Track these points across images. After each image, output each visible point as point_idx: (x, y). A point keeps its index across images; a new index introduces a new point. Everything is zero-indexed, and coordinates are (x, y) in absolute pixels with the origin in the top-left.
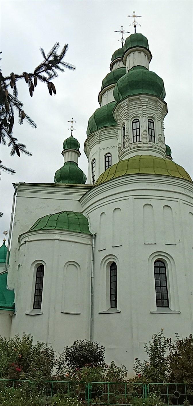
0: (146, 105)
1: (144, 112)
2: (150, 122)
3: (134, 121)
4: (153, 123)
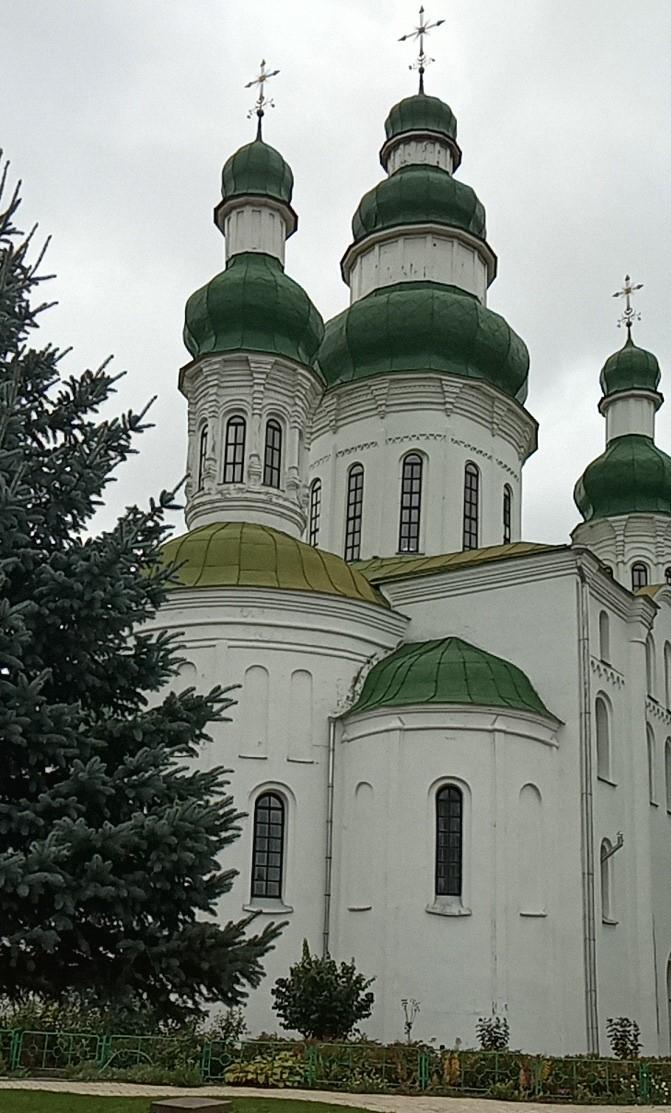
0: (263, 382)
1: (256, 401)
2: (272, 427)
3: (232, 421)
4: (280, 431)
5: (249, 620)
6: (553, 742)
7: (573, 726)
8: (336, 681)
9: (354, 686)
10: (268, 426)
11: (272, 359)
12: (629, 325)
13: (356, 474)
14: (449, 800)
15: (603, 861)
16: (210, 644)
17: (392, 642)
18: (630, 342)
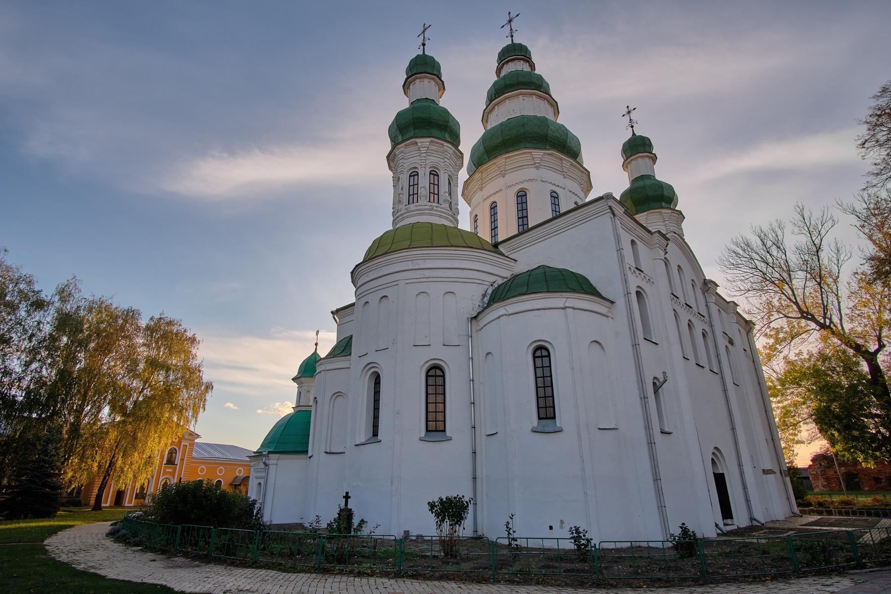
5: (417, 267)
6: (609, 314)
7: (621, 303)
8: (471, 296)
9: (483, 299)
10: (430, 173)
11: (429, 140)
12: (632, 127)
13: (493, 207)
14: (541, 353)
15: (656, 391)
16: (395, 284)
17: (508, 274)
18: (634, 134)
